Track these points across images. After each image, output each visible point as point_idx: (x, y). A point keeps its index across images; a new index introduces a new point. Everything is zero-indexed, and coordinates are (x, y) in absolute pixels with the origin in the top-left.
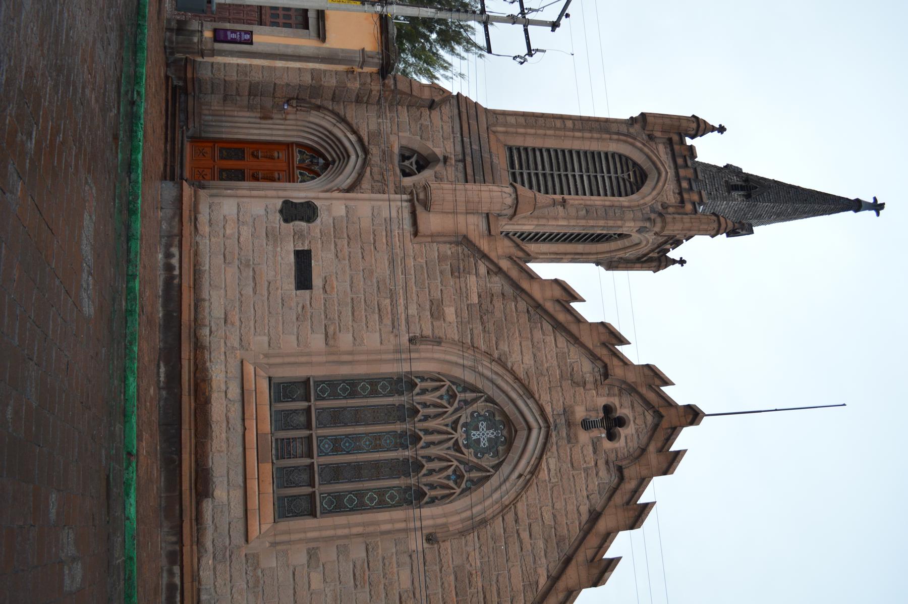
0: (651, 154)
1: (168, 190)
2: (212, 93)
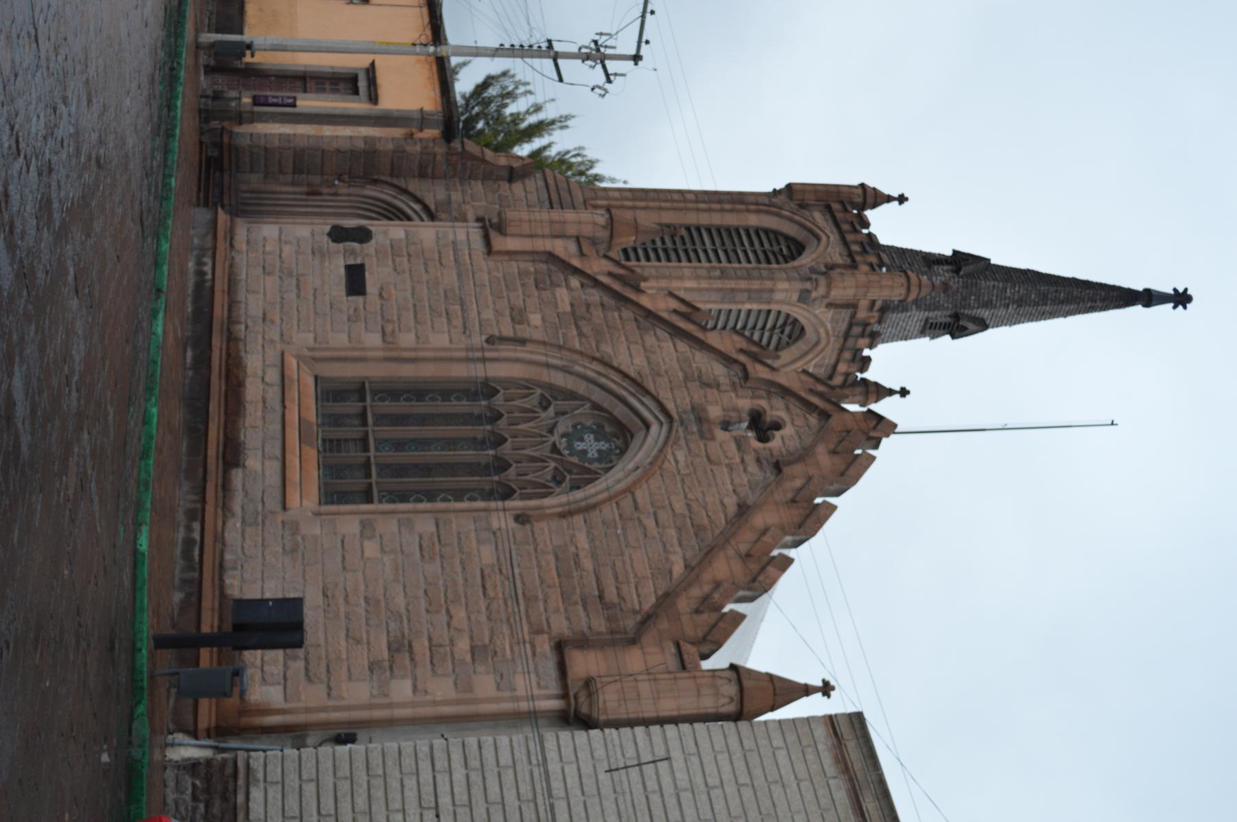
0: (803, 221)
1: (203, 215)
2: (251, 171)
